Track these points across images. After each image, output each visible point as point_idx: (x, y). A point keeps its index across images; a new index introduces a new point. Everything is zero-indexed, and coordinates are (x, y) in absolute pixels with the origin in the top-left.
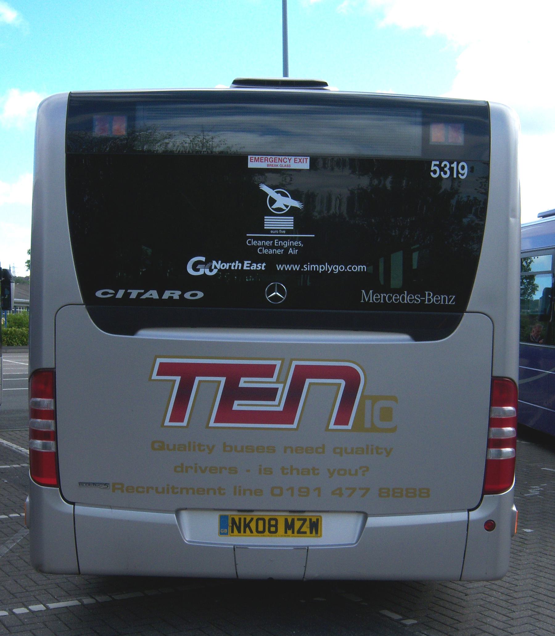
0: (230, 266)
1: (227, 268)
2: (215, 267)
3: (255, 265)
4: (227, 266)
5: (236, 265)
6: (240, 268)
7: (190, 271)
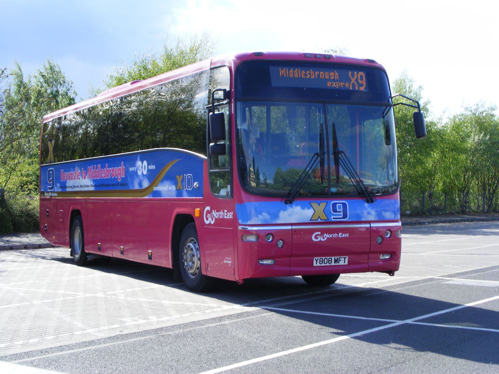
0: (332, 236)
2: (326, 237)
3: (344, 234)
4: (331, 236)
7: (314, 239)
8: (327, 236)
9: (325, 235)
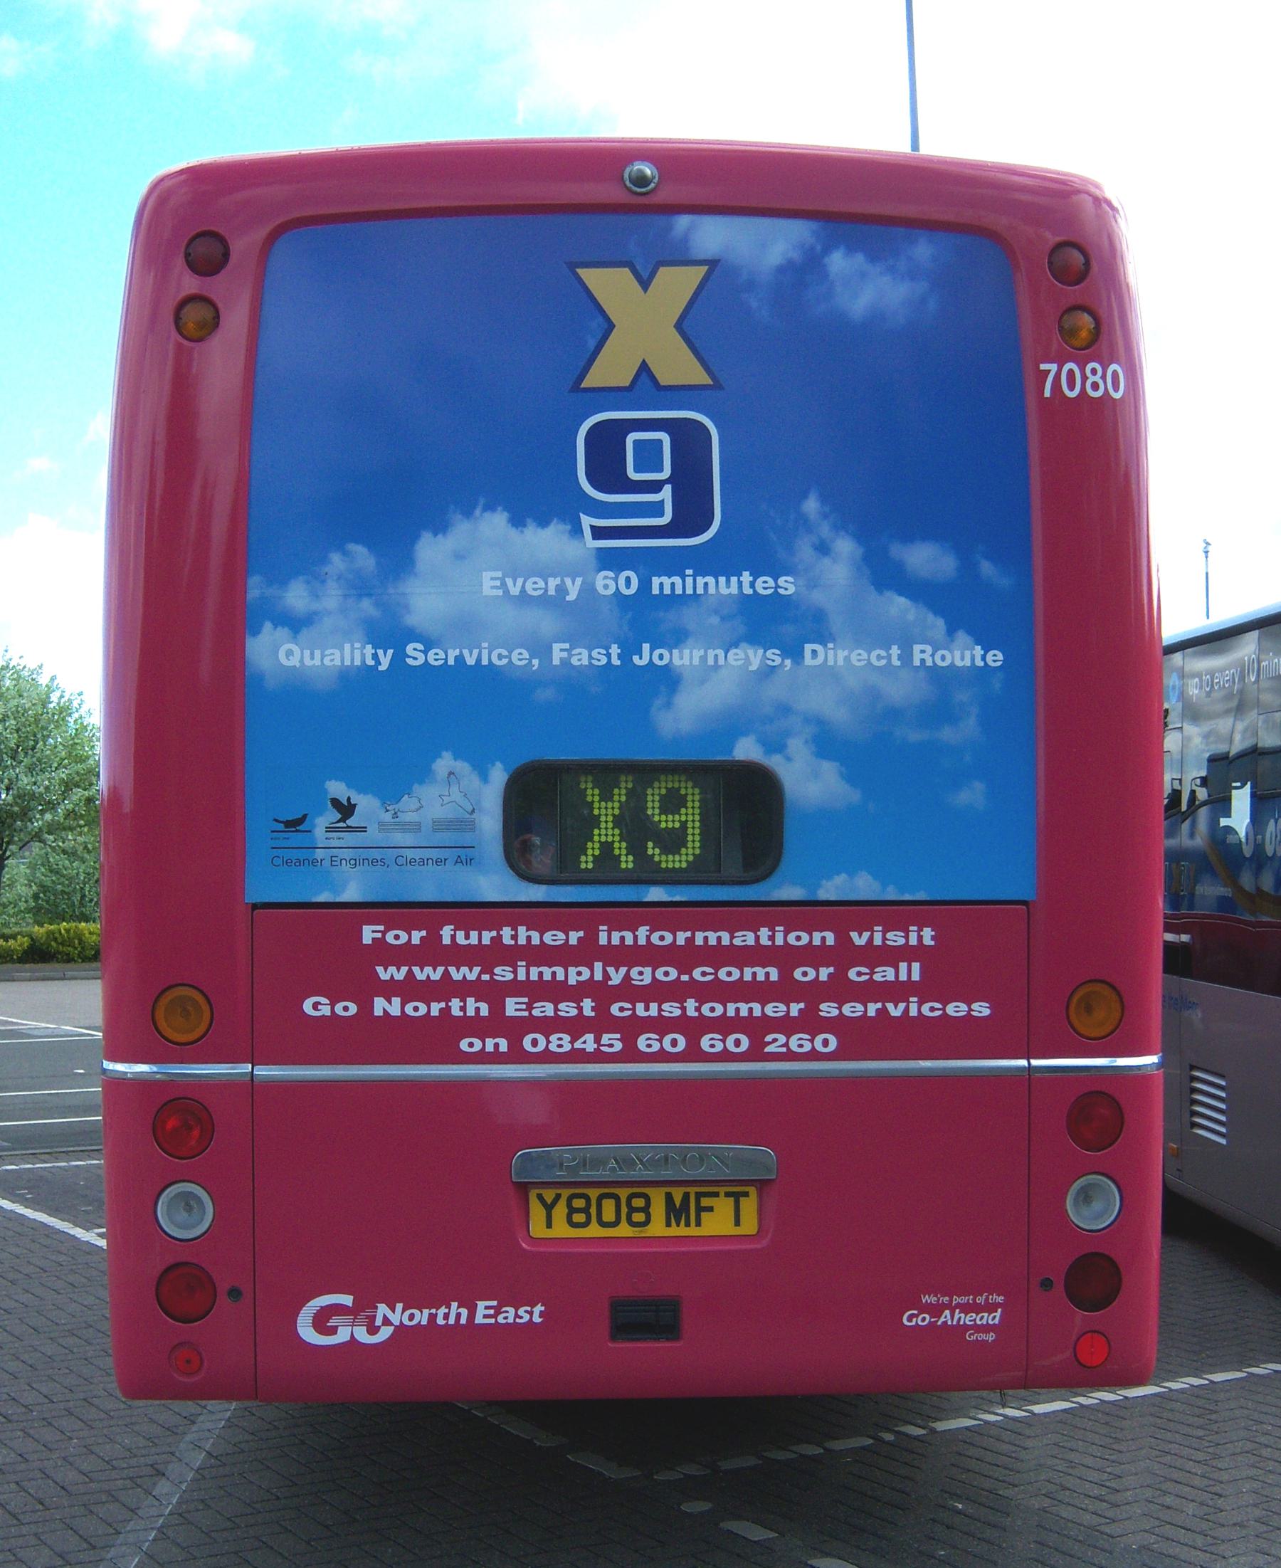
0: (432, 1318)
1: (424, 1322)
2: (386, 1322)
3: (511, 1310)
4: (422, 1317)
5: (452, 1313)
6: (463, 1321)
7: (307, 1333)
8: (395, 1318)
9: (382, 1309)
